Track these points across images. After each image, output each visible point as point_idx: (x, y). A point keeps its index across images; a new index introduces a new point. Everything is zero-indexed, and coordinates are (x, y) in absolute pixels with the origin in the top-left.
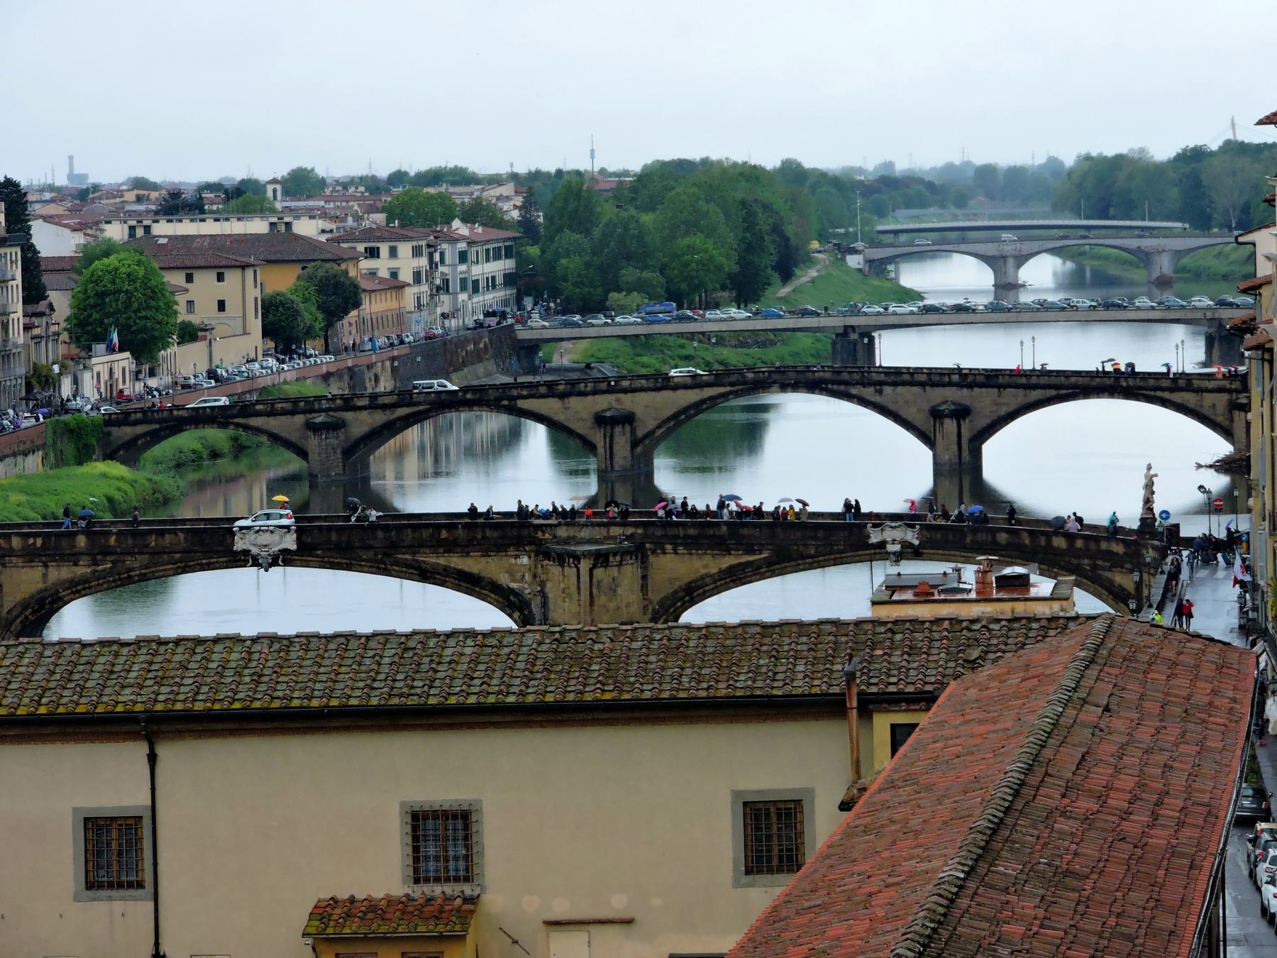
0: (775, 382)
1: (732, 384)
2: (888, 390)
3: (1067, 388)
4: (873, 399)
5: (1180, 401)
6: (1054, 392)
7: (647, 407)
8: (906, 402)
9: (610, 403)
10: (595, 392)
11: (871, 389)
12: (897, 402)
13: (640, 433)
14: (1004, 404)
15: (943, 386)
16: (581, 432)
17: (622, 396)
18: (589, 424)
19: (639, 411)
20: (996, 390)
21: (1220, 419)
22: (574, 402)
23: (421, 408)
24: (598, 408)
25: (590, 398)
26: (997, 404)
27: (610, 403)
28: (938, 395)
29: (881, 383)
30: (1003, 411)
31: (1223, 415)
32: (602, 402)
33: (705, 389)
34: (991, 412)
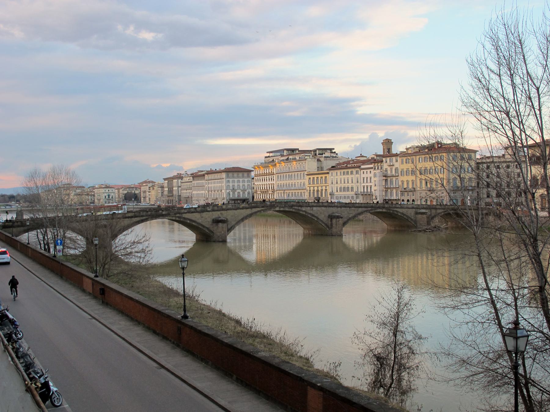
0: (278, 206)
1: (263, 207)
2: (315, 208)
3: (370, 207)
4: (310, 212)
5: (402, 212)
6: (366, 209)
7: (232, 216)
8: (321, 213)
9: (218, 215)
10: (213, 210)
11: (309, 208)
12: (318, 213)
13: (229, 227)
14: (351, 213)
15: (332, 207)
16: (207, 226)
17: (223, 212)
18: (211, 223)
19: (229, 218)
20: (349, 208)
21: (413, 218)
22: (205, 214)
23: (144, 218)
24: (214, 217)
25: (211, 213)
26: (349, 214)
27: (218, 215)
28: (331, 210)
29: (313, 206)
30: (351, 216)
31: (413, 216)
32: (216, 215)
33: (253, 209)
34: (347, 216)
